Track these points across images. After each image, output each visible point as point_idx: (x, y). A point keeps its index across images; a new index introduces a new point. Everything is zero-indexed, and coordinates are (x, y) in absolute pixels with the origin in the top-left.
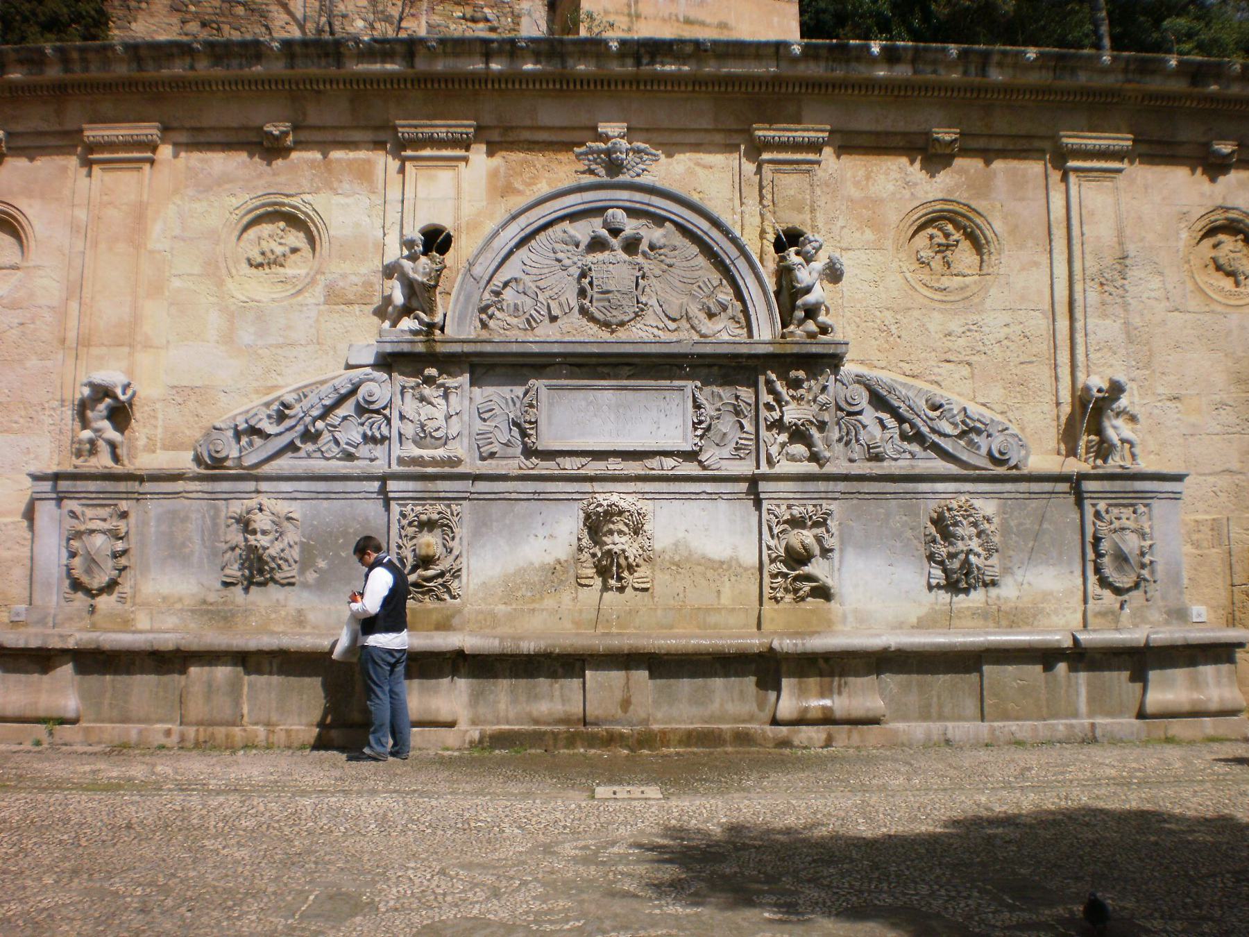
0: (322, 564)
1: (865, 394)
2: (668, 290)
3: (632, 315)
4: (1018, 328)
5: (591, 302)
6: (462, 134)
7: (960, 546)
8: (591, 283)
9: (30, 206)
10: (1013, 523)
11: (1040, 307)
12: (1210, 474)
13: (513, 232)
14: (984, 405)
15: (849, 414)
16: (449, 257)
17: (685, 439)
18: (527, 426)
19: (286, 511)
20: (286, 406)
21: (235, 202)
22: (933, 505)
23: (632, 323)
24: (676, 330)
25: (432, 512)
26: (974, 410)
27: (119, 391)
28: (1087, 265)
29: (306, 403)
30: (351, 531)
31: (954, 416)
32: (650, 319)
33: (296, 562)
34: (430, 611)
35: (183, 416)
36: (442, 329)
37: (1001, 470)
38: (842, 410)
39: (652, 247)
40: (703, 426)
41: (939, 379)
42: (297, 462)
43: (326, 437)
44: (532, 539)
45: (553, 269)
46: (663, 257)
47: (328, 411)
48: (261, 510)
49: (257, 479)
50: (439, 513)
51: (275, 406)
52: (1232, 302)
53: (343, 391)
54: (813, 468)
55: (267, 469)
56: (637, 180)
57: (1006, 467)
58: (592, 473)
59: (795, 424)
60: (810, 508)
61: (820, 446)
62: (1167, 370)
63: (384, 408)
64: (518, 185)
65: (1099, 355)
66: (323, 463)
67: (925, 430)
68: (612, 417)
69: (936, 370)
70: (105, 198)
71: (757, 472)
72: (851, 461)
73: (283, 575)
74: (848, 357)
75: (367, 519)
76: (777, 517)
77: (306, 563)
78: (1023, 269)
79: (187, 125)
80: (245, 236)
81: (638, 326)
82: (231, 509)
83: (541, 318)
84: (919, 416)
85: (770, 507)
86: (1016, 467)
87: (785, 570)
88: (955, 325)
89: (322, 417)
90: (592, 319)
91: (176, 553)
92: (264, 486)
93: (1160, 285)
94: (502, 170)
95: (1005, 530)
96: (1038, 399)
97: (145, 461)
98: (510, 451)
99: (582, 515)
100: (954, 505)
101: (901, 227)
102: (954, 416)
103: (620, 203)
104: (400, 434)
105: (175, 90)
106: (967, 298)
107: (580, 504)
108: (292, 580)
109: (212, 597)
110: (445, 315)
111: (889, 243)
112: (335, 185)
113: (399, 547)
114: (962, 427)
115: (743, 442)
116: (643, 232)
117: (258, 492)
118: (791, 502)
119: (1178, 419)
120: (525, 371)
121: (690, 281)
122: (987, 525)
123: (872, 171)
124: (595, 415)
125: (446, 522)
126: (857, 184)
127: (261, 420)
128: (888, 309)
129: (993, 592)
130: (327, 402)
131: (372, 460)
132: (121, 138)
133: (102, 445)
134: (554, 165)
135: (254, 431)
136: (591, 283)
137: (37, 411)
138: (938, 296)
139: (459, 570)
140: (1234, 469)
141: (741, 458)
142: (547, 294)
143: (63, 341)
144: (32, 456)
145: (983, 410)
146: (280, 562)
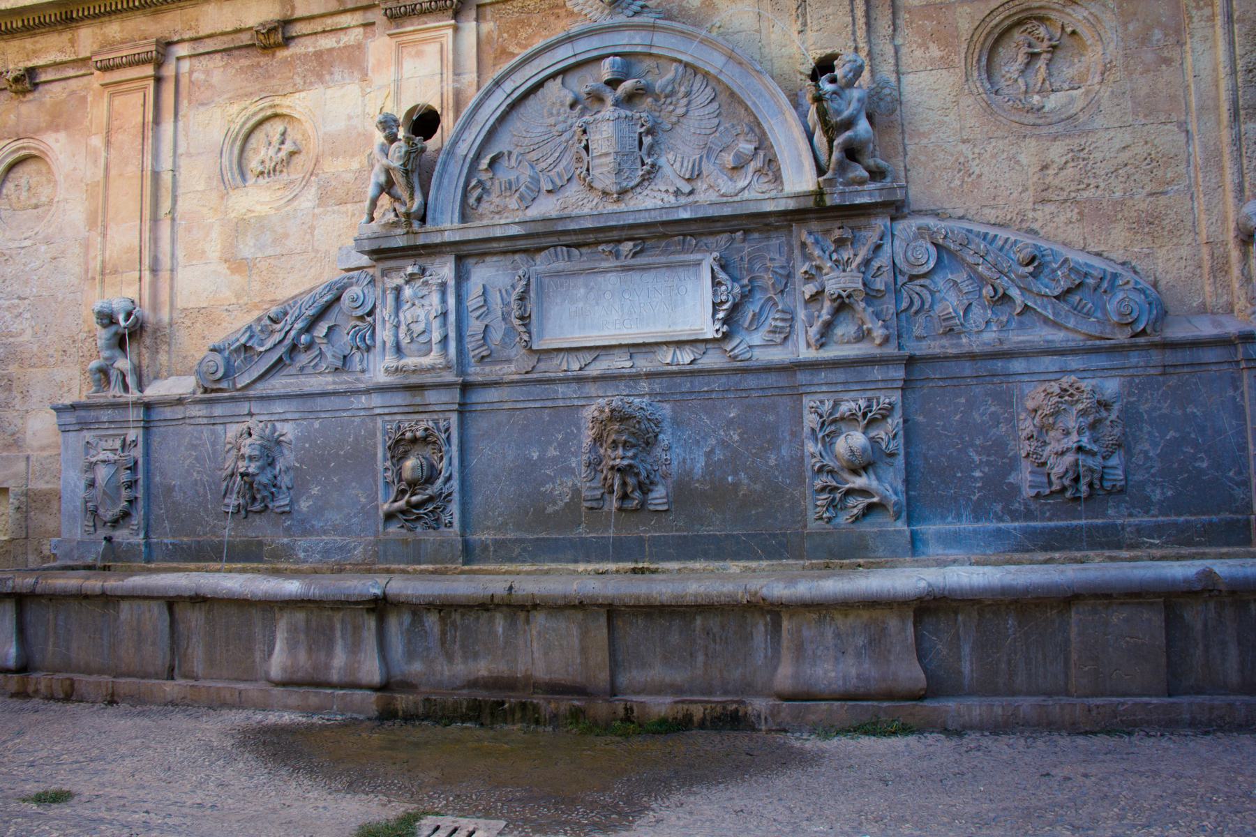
3: (638, 180)
4: (1140, 150)
5: (588, 170)
8: (586, 148)
9: (57, 141)
10: (1143, 408)
13: (498, 102)
14: (1099, 254)
15: (912, 278)
19: (276, 434)
23: (638, 190)
24: (691, 193)
26: (1079, 258)
27: (121, 318)
31: (1054, 271)
37: (1122, 337)
40: (726, 306)
41: (1036, 226)
48: (250, 435)
49: (249, 399)
50: (426, 430)
55: (260, 389)
57: (1129, 331)
59: (840, 296)
63: (370, 313)
64: (512, 49)
67: (1014, 293)
73: (277, 504)
76: (821, 417)
79: (186, 36)
85: (812, 404)
86: (1143, 332)
88: (1057, 152)
94: (495, 35)
95: (1130, 417)
96: (1175, 240)
97: (154, 391)
102: (1054, 271)
103: (618, 50)
111: (959, 60)
112: (327, 77)
114: (1064, 285)
117: (251, 414)
118: (841, 396)
122: (1104, 414)
128: (963, 142)
133: (114, 374)
138: (1031, 118)
139: (450, 494)
141: (776, 345)
145: (1096, 262)
146: (274, 490)
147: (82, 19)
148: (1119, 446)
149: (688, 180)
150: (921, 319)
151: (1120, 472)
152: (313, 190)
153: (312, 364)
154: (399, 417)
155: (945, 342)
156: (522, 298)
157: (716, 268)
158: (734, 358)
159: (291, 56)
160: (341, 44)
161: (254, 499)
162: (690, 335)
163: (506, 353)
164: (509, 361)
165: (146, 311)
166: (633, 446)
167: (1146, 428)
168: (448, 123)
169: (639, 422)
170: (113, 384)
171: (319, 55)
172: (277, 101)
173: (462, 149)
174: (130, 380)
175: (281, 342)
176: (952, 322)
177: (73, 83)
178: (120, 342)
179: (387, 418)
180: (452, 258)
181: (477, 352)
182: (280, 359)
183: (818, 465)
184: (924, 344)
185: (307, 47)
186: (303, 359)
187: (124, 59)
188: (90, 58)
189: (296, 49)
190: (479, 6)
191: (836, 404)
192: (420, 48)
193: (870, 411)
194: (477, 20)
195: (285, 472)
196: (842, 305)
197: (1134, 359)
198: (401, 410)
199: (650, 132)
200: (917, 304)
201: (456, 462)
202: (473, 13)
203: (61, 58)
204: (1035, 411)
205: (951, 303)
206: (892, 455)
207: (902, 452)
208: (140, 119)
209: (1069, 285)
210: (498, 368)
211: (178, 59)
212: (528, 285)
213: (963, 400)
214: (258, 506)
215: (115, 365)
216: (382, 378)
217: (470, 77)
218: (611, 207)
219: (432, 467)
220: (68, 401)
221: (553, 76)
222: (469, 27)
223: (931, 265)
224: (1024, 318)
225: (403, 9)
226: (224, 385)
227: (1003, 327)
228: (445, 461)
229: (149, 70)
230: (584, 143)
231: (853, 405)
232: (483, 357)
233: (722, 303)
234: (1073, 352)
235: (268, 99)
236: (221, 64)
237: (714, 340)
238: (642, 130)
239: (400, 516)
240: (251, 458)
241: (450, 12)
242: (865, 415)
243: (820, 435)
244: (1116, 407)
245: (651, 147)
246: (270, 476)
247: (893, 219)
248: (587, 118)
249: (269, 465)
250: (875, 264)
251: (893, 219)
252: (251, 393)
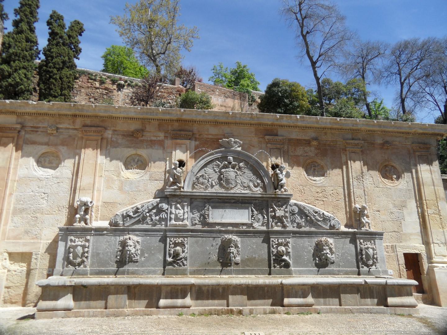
0: (146, 255)
2: (244, 179)
8: (223, 177)
9: (63, 149)
20: (138, 209)
25: (179, 240)
32: (239, 186)
33: (139, 254)
48: (130, 239)
50: (181, 240)
52: (392, 185)
59: (279, 217)
60: (284, 240)
63: (166, 210)
65: (357, 199)
73: (135, 259)
77: (142, 254)
81: (236, 188)
82: (120, 239)
107: (220, 238)
112: (153, 147)
126: (292, 152)
136: (223, 177)
137: (62, 209)
140: (396, 231)
142: (212, 179)
159: (143, 139)
160: (158, 139)
171: (151, 141)
185: (148, 138)
190: (195, 138)
202: (194, 139)
211: (108, 134)
225: (177, 135)
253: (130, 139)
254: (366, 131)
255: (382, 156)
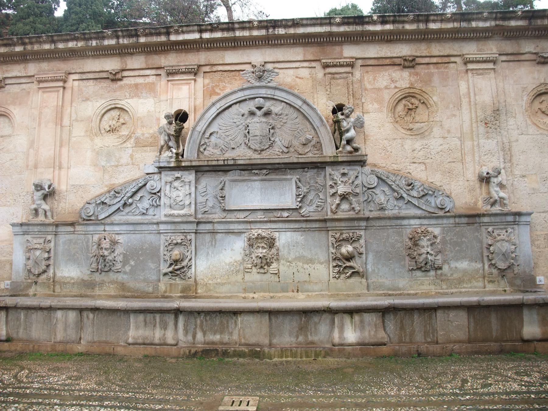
0: (132, 263)
1: (376, 179)
3: (268, 146)
5: (249, 141)
6: (192, 69)
7: (423, 251)
8: (248, 132)
9: (15, 109)
11: (457, 135)
12: (543, 212)
13: (213, 111)
16: (186, 125)
17: (292, 203)
18: (221, 199)
21: (98, 104)
22: (409, 231)
23: (268, 150)
24: (288, 152)
28: (478, 114)
29: (124, 192)
30: (145, 248)
34: (178, 284)
35: (76, 198)
36: (182, 156)
37: (441, 213)
38: (366, 187)
39: (276, 114)
40: (301, 196)
42: (122, 217)
43: (134, 206)
44: (224, 251)
45: (232, 127)
46: (281, 119)
47: (135, 193)
48: (105, 239)
49: (104, 224)
50: (182, 239)
51: (113, 193)
53: (140, 185)
54: (352, 214)
55: (108, 221)
56: (269, 84)
57: (444, 211)
58: (251, 220)
59: (343, 194)
61: (355, 205)
62: (519, 163)
63: (158, 192)
64: (217, 91)
65: (486, 157)
66: (133, 217)
67: (405, 195)
68: (259, 194)
69: (409, 167)
70: (44, 104)
71: (326, 217)
72: (371, 211)
73: (115, 268)
74: (368, 162)
75: (151, 243)
76: (336, 239)
77: (125, 262)
78: (448, 118)
79: (78, 71)
80: (103, 119)
83: (227, 149)
84: (402, 189)
85: (332, 234)
86: (449, 211)
87: (340, 264)
89: (131, 197)
90: (250, 148)
91: (72, 259)
92: (108, 228)
93: (514, 123)
95: (444, 241)
98: (214, 211)
99: (246, 239)
100: (419, 231)
101: (390, 102)
102: (418, 188)
103: (261, 96)
104: (165, 204)
105: (72, 56)
106: (422, 133)
107: (246, 235)
108: (120, 270)
109: (86, 278)
110: (184, 150)
113: (165, 255)
114: (422, 193)
115: (320, 203)
116: (272, 108)
117: (105, 231)
119: (525, 186)
120: (220, 173)
121: (293, 129)
123: (376, 76)
124: (251, 193)
125: (185, 243)
127: (106, 199)
129: (439, 272)
130: (134, 190)
131: (154, 215)
132: (50, 78)
133: (41, 211)
134: (233, 81)
135: (103, 203)
136: (248, 132)
137: (17, 197)
139: (191, 266)
143: (27, 166)
144: (15, 216)
146: (114, 262)
147: (31, 60)
148: (440, 252)
149: (287, 148)
150: (372, 204)
151: (440, 261)
152: (132, 140)
153: (133, 211)
154: (170, 234)
155: (379, 212)
156: (222, 189)
157: (298, 182)
158: (303, 216)
160: (146, 82)
161: (105, 266)
162: (287, 206)
163: (214, 211)
164: (215, 213)
165: (55, 185)
166: (265, 248)
167: (449, 246)
168: (191, 118)
169: (268, 239)
170: (40, 215)
171: (136, 86)
172: (117, 102)
173: (198, 128)
174: (49, 214)
175: (119, 201)
176: (383, 206)
177: (24, 86)
178: (45, 197)
179: (165, 234)
180: (194, 171)
181: (203, 209)
182: (119, 208)
183: (334, 257)
184: (372, 213)
186: (127, 209)
187: (50, 78)
188: (34, 76)
189: (126, 81)
191: (341, 234)
192: (180, 86)
193: (354, 237)
194: (203, 77)
195: (119, 255)
196: (344, 197)
197: (445, 221)
198: (171, 231)
199: (273, 128)
200: (370, 198)
201: (193, 253)
202: (202, 74)
203: (19, 74)
204: (411, 239)
205: (382, 198)
206: (361, 254)
207: (364, 253)
208: (55, 103)
209: (423, 193)
210: (211, 216)
212: (224, 184)
213: (386, 234)
214: (106, 269)
215: (42, 207)
216: (163, 219)
217: (200, 101)
218: (256, 156)
219: (184, 254)
220: (15, 221)
221: (236, 103)
222: (200, 80)
223: (376, 184)
224: (407, 205)
225: (174, 70)
226: (93, 218)
227: (400, 208)
228: (190, 252)
229: (61, 84)
230: (248, 130)
231: (347, 235)
232: (205, 212)
233: (299, 195)
234: (425, 218)
235: (113, 101)
236: (93, 84)
237: (296, 209)
238: (270, 127)
239: (170, 274)
240: (106, 249)
241: (193, 74)
242: (352, 239)
243: (335, 246)
244: (439, 238)
245: (273, 134)
246: (113, 257)
247: (362, 166)
248: (248, 121)
249: (112, 252)
250: (356, 183)
251: (362, 166)
252: (103, 222)
253: (105, 85)
254: (497, 34)
255: (534, 78)
